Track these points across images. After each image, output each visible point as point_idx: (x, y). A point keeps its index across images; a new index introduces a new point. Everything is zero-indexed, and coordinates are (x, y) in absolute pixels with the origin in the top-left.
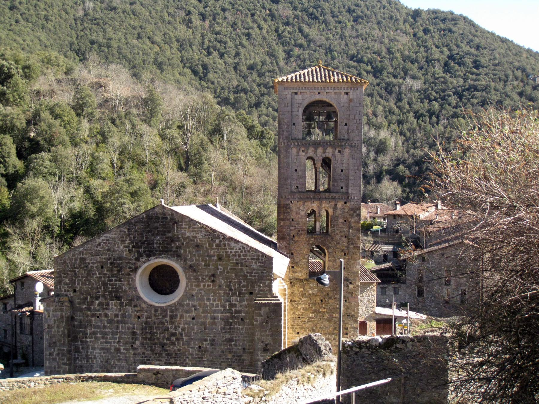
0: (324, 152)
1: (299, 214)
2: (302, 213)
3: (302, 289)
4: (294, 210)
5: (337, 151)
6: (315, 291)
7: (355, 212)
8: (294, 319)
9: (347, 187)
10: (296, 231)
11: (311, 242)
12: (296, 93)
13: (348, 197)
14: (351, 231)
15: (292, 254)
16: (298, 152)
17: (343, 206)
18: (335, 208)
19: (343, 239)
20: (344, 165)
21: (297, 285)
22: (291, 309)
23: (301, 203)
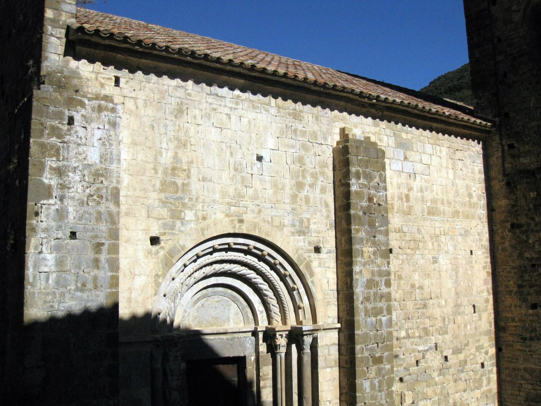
2: (517, 17)
3: (533, 195)
8: (522, 271)
15: (507, 115)
22: (514, 247)
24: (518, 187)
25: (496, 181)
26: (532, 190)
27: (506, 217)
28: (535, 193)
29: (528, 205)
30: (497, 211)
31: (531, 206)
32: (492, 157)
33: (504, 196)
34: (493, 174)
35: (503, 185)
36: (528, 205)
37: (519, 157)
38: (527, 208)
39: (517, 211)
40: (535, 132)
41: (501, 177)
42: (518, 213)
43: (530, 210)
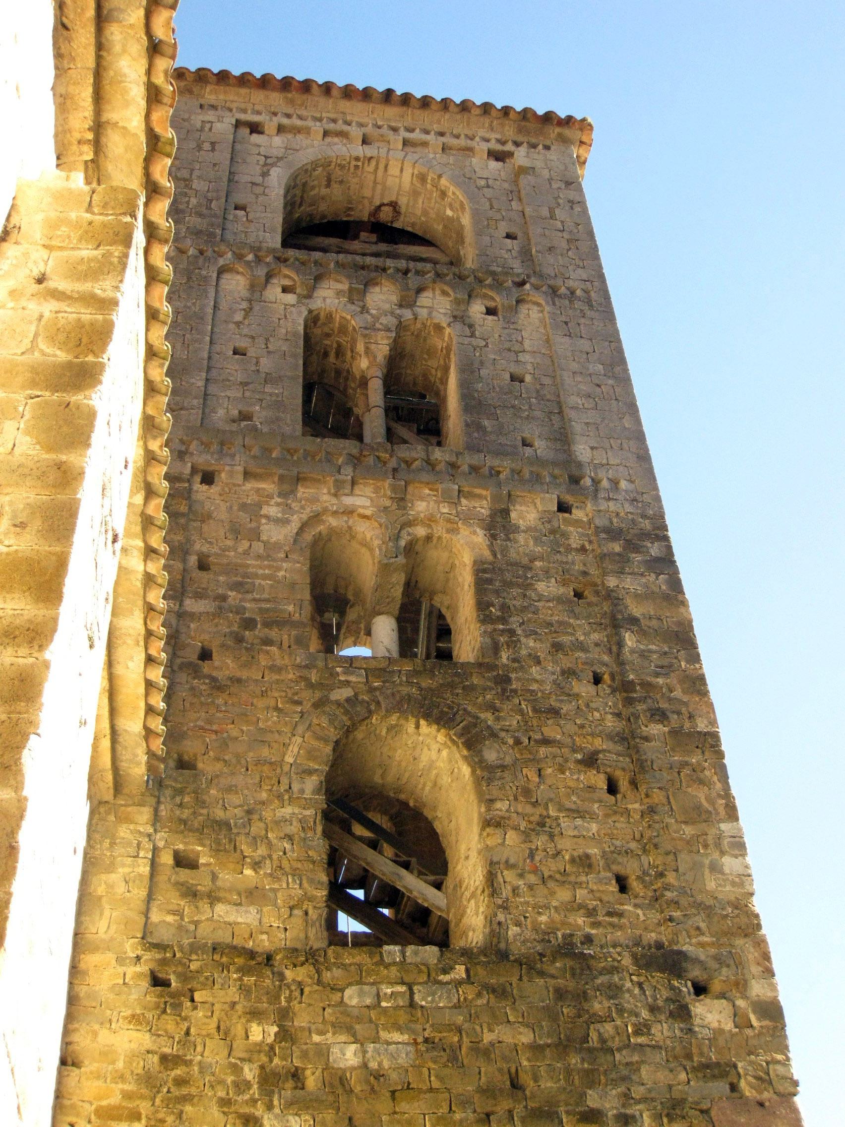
0: (407, 302)
1: (255, 535)
3: (261, 1033)
4: (222, 513)
5: (477, 309)
6: (394, 1051)
7: (632, 546)
9: (563, 438)
10: (229, 625)
11: (341, 694)
12: (255, 128)
13: (575, 480)
14: (630, 640)
16: (257, 288)
17: (545, 518)
18: (499, 524)
19: (584, 688)
20: (524, 358)
21: (219, 996)
23: (268, 486)
24: (197, 996)
25: (110, 957)
26: (255, 1015)
27: (127, 1096)
28: (275, 1029)
29: (235, 1066)
30: (90, 1066)
31: (250, 1073)
32: (111, 868)
33: (135, 1019)
34: (102, 927)
35: (139, 975)
36: (236, 1069)
37: (213, 898)
38: (230, 1079)
39: (180, 1082)
40: (290, 838)
41: (131, 948)
42: (185, 1091)
43: (242, 1086)
